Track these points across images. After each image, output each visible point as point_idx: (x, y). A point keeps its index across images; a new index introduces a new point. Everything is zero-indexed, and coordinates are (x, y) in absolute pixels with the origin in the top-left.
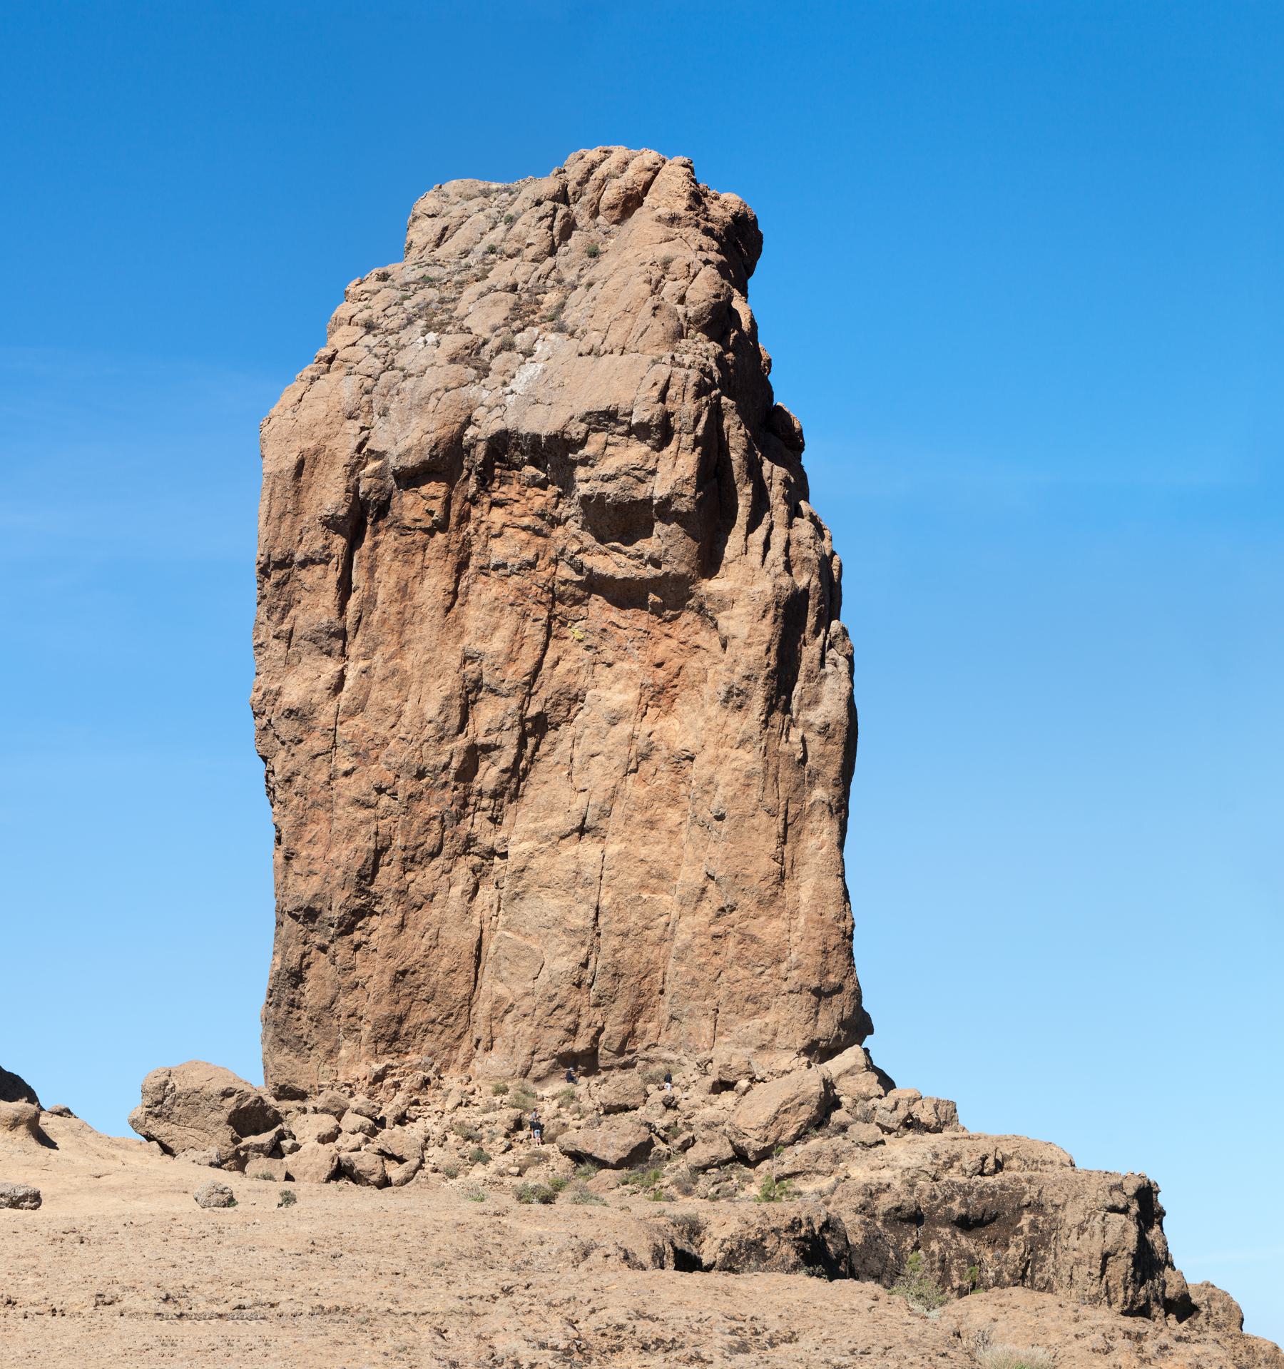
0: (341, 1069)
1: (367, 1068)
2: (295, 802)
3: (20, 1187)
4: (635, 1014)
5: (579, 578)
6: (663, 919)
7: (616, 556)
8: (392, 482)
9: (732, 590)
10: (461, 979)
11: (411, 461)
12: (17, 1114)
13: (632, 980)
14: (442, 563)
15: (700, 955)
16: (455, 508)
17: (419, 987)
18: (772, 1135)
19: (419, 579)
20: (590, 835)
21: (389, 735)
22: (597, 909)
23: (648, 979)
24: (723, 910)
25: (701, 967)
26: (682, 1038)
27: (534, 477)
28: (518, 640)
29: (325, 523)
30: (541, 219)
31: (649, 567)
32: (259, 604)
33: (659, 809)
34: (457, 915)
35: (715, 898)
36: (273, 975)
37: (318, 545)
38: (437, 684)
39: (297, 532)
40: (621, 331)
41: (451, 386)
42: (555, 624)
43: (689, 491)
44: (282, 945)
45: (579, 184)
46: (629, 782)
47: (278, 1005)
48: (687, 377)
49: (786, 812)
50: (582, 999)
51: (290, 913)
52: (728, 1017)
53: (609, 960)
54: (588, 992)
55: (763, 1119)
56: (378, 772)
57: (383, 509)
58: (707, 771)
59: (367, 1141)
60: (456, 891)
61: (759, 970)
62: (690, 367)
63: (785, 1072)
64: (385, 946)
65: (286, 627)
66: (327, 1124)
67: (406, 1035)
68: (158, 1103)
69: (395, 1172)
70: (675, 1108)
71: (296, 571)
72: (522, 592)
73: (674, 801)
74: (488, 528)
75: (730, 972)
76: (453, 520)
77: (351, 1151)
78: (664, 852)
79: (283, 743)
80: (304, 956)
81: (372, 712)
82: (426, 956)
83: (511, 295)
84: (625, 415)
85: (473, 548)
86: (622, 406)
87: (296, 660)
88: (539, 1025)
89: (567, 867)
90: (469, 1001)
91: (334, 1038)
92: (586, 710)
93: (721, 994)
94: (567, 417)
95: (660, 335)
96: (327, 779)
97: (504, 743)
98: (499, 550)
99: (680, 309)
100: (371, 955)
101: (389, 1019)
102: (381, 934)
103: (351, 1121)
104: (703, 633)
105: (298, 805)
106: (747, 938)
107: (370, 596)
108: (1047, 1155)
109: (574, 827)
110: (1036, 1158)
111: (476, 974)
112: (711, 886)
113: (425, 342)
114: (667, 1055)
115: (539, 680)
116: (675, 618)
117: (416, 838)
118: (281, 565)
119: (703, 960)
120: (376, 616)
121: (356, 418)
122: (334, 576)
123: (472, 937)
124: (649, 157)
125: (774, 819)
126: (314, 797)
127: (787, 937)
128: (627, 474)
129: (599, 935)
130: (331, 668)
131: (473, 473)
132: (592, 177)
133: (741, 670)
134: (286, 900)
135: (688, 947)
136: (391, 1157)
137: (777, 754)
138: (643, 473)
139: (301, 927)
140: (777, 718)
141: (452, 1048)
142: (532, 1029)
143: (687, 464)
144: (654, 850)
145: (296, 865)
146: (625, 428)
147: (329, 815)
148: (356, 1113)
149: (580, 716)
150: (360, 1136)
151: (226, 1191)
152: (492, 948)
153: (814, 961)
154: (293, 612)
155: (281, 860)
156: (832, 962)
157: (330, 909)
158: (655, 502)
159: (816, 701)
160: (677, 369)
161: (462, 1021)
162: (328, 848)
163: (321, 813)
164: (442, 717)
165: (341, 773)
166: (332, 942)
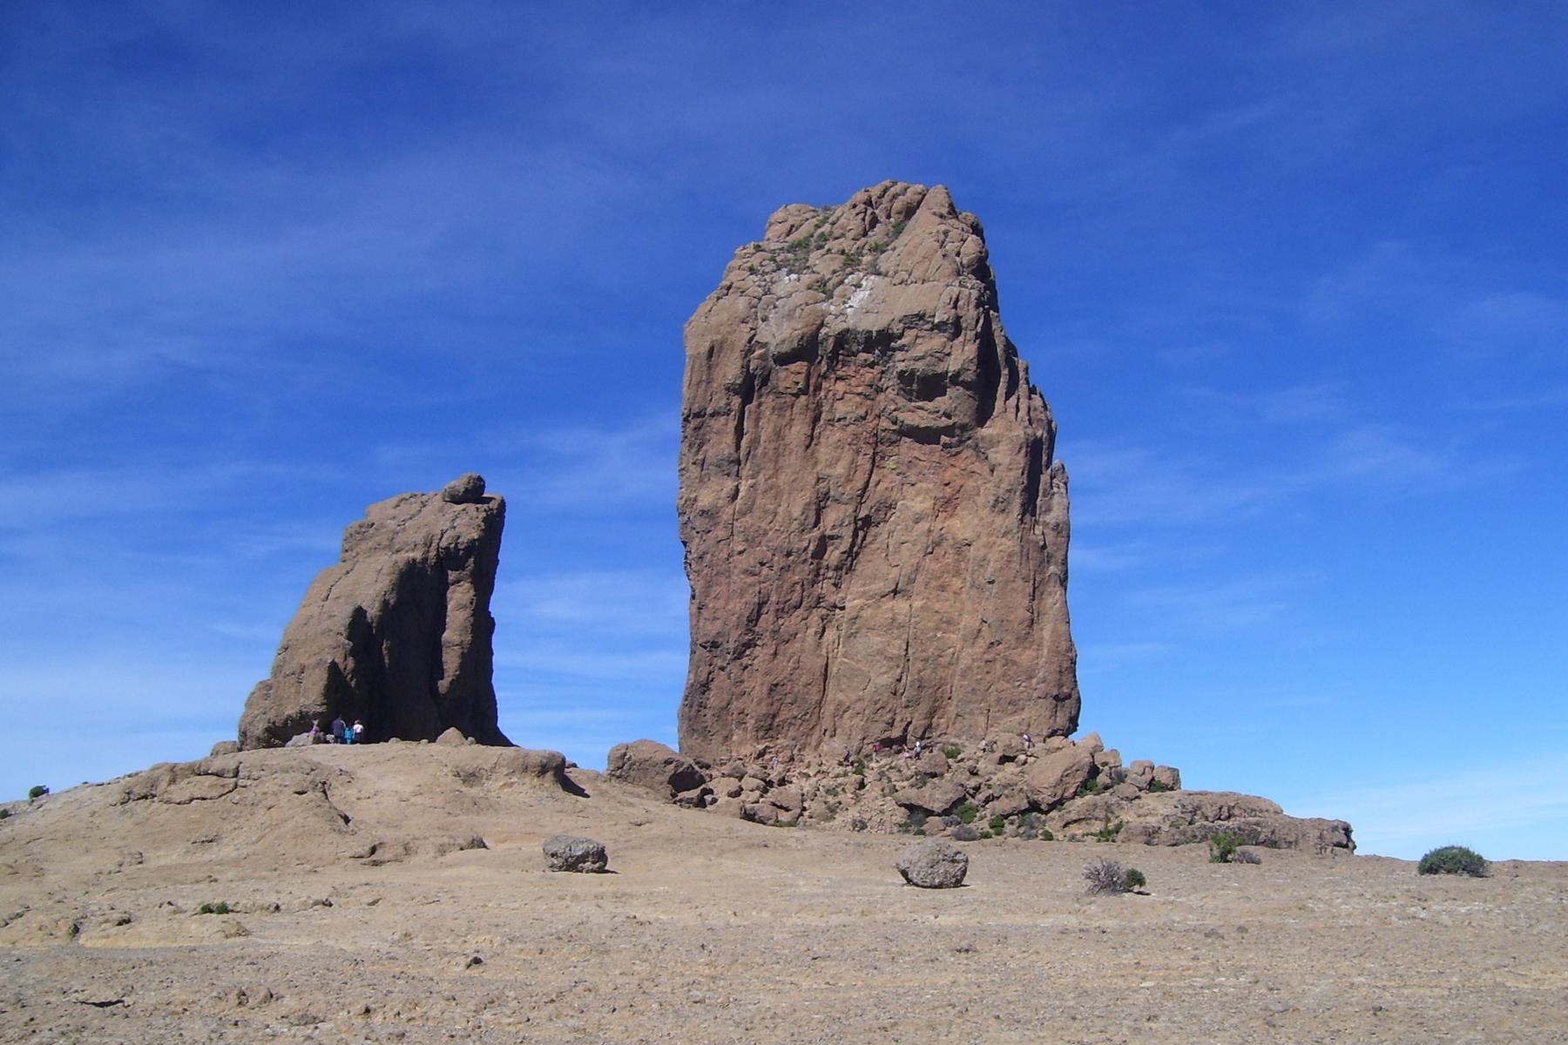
0: (734, 749)
1: (750, 749)
2: (705, 572)
3: (578, 842)
4: (931, 714)
5: (894, 427)
6: (951, 650)
7: (920, 412)
8: (772, 362)
9: (998, 435)
10: (815, 689)
11: (785, 348)
12: (545, 761)
13: (931, 690)
14: (803, 417)
15: (978, 674)
16: (813, 381)
17: (786, 694)
18: (1059, 792)
19: (788, 427)
20: (901, 595)
21: (768, 528)
22: (908, 643)
23: (940, 690)
24: (992, 643)
25: (978, 682)
26: (965, 729)
27: (866, 360)
28: (853, 467)
29: (728, 389)
30: (857, 214)
31: (943, 418)
32: (682, 442)
33: (947, 578)
34: (812, 647)
35: (987, 635)
36: (688, 686)
37: (723, 403)
38: (800, 495)
39: (709, 394)
40: (921, 269)
41: (810, 302)
42: (878, 458)
43: (973, 368)
44: (694, 666)
45: (879, 198)
46: (927, 560)
47: (691, 706)
48: (970, 294)
49: (1035, 580)
50: (893, 703)
51: (700, 645)
52: (998, 714)
53: (916, 677)
54: (901, 699)
55: (1052, 781)
56: (762, 552)
57: (765, 381)
58: (982, 553)
59: (762, 796)
60: (811, 631)
61: (1018, 684)
62: (971, 289)
63: (1058, 749)
64: (764, 667)
65: (700, 457)
66: (733, 784)
67: (778, 726)
68: (619, 768)
69: (784, 817)
70: (976, 774)
71: (707, 421)
72: (856, 436)
73: (957, 573)
74: (834, 395)
75: (998, 685)
76: (811, 389)
77: (753, 803)
78: (951, 606)
79: (698, 533)
80: (710, 673)
81: (757, 513)
82: (792, 674)
83: (841, 256)
84: (930, 317)
85: (824, 408)
86: (928, 311)
87: (706, 479)
88: (868, 719)
89: (886, 616)
90: (820, 704)
91: (728, 728)
92: (898, 514)
93: (992, 699)
94: (890, 319)
95: (950, 270)
96: (726, 556)
97: (844, 534)
98: (841, 409)
99: (958, 259)
100: (755, 673)
101: (766, 716)
102: (761, 659)
103: (748, 782)
104: (977, 463)
105: (707, 574)
106: (1008, 662)
107: (755, 438)
108: (1263, 806)
109: (891, 590)
110: (1255, 808)
111: (825, 686)
112: (985, 628)
113: (790, 280)
114: (953, 740)
115: (867, 494)
116: (958, 453)
117: (785, 596)
118: (697, 415)
119: (979, 677)
120: (760, 450)
121: (747, 323)
122: (732, 424)
123: (821, 662)
124: (920, 187)
125: (1027, 584)
126: (719, 568)
127: (1036, 661)
128: (931, 355)
129: (908, 660)
130: (730, 484)
131: (825, 358)
132: (887, 194)
133: (1004, 486)
134: (699, 636)
135: (969, 668)
136: (781, 807)
137: (1028, 541)
138: (942, 355)
139: (708, 654)
140: (1028, 518)
141: (808, 735)
142: (862, 723)
143: (971, 350)
144: (944, 605)
145: (705, 614)
146: (930, 326)
147: (728, 580)
148: (753, 777)
149: (892, 519)
150: (757, 793)
151: (958, 857)
152: (835, 669)
153: (1053, 678)
154: (705, 448)
155: (695, 610)
156: (1064, 678)
157: (728, 642)
158: (950, 374)
159: (1049, 510)
160: (963, 289)
161: (815, 717)
162: (727, 602)
163: (723, 579)
164: (803, 518)
165: (736, 553)
166: (728, 664)
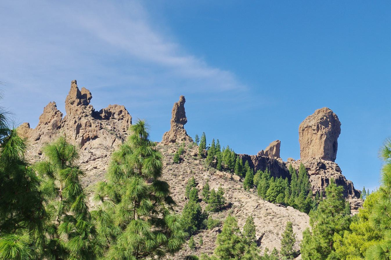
56: (304, 143)
